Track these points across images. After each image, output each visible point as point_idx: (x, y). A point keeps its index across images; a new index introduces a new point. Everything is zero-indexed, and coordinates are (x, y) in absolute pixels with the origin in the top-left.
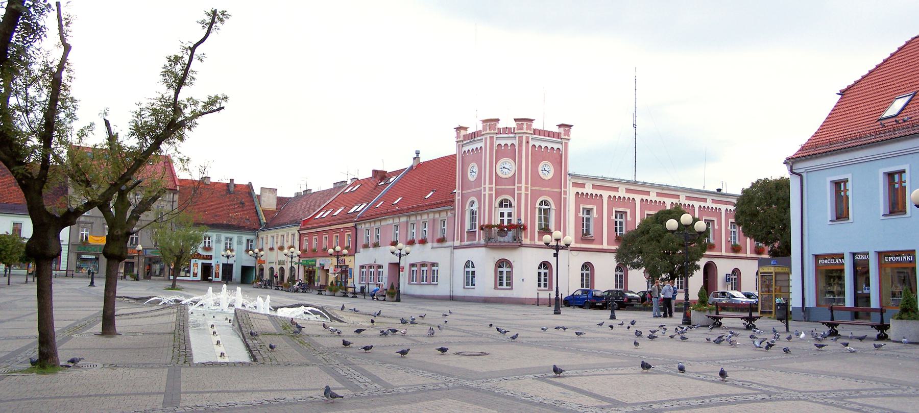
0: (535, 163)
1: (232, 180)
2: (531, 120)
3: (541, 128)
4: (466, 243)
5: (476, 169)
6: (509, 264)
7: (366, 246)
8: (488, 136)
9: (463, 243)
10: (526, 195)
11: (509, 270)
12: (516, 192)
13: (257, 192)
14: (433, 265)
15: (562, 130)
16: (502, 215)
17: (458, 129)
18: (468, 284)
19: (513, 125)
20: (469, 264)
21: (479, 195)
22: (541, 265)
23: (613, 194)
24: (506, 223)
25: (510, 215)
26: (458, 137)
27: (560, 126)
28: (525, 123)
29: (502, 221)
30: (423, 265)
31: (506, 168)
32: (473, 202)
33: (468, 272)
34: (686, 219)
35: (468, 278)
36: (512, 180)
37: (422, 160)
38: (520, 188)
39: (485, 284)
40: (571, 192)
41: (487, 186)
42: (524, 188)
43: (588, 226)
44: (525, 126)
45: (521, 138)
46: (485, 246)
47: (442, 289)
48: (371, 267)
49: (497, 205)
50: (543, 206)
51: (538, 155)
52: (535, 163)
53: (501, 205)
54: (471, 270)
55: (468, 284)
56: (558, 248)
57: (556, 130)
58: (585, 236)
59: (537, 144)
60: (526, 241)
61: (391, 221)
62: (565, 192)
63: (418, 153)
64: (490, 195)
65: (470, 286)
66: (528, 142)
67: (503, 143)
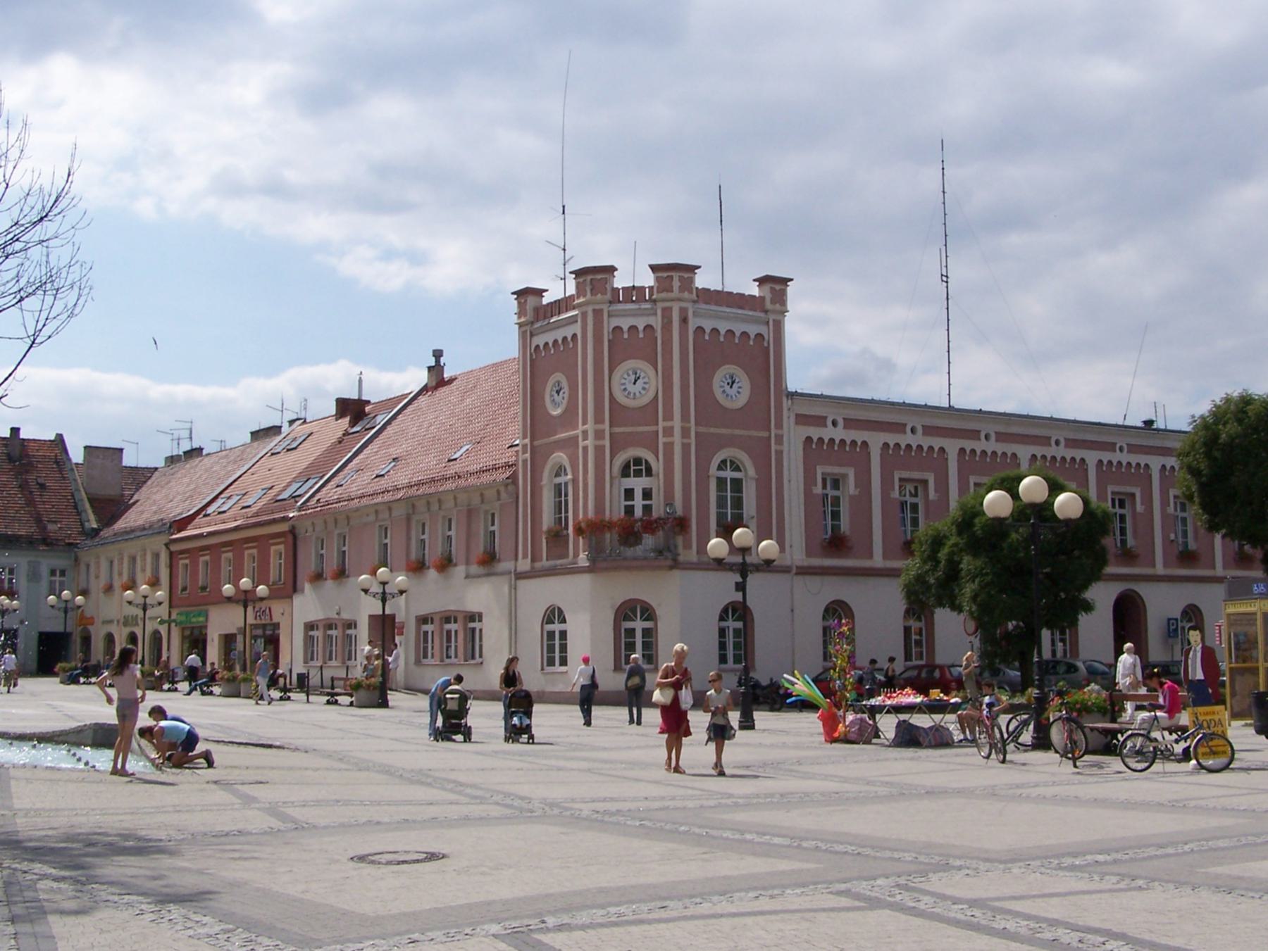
0: (705, 369)
1: (15, 431)
2: (692, 269)
3: (715, 285)
4: (545, 563)
6: (648, 613)
7: (318, 577)
8: (590, 309)
9: (538, 565)
10: (686, 447)
11: (648, 624)
12: (661, 440)
13: (77, 455)
16: (629, 494)
17: (522, 294)
18: (551, 662)
19: (647, 280)
20: (554, 615)
22: (725, 610)
23: (892, 439)
24: (638, 512)
25: (647, 494)
26: (520, 314)
27: (762, 281)
29: (629, 510)
31: (636, 384)
32: (560, 471)
33: (551, 635)
34: (1032, 486)
35: (551, 649)
38: (669, 432)
40: (793, 439)
41: (590, 427)
42: (676, 430)
43: (836, 515)
44: (676, 284)
45: (667, 312)
48: (330, 627)
50: (729, 474)
51: (711, 351)
52: (705, 369)
53: (625, 471)
54: (556, 627)
56: (744, 570)
57: (754, 290)
59: (708, 325)
62: (779, 439)
63: (438, 354)
64: (599, 450)
66: (684, 320)
67: (625, 323)
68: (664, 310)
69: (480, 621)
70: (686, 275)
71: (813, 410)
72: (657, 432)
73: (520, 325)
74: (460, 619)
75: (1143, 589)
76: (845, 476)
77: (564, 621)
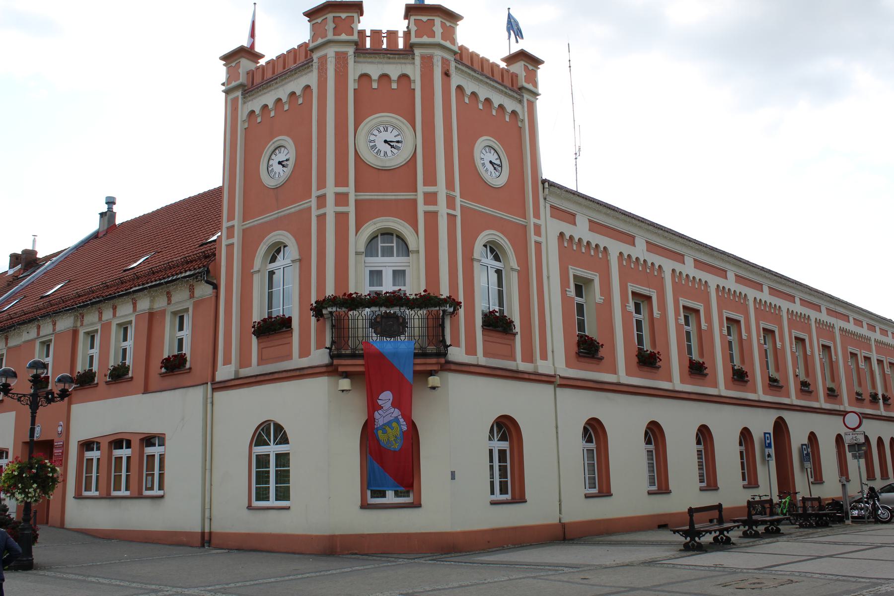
5: (288, 153)
9: (245, 372)
10: (451, 218)
12: (421, 208)
14: (149, 440)
15: (518, 68)
19: (401, 26)
21: (299, 226)
25: (399, 275)
28: (438, 21)
30: (118, 443)
31: (383, 140)
32: (276, 250)
33: (263, 461)
35: (262, 478)
36: (404, 175)
37: (119, 221)
38: (431, 198)
39: (328, 491)
40: (550, 230)
41: (331, 190)
42: (442, 197)
44: (438, 29)
45: (427, 62)
46: (331, 370)
47: (177, 508)
49: (362, 248)
53: (371, 248)
54: (272, 449)
55: (262, 495)
58: (587, 349)
60: (457, 354)
61: (33, 334)
62: (537, 228)
63: (111, 202)
64: (341, 218)
65: (272, 502)
66: (447, 74)
68: (423, 57)
69: (162, 444)
70: (448, 24)
71: (569, 202)
72: (414, 202)
73: (227, 92)
74: (135, 443)
75: (788, 416)
76: (589, 281)
77: (285, 440)
